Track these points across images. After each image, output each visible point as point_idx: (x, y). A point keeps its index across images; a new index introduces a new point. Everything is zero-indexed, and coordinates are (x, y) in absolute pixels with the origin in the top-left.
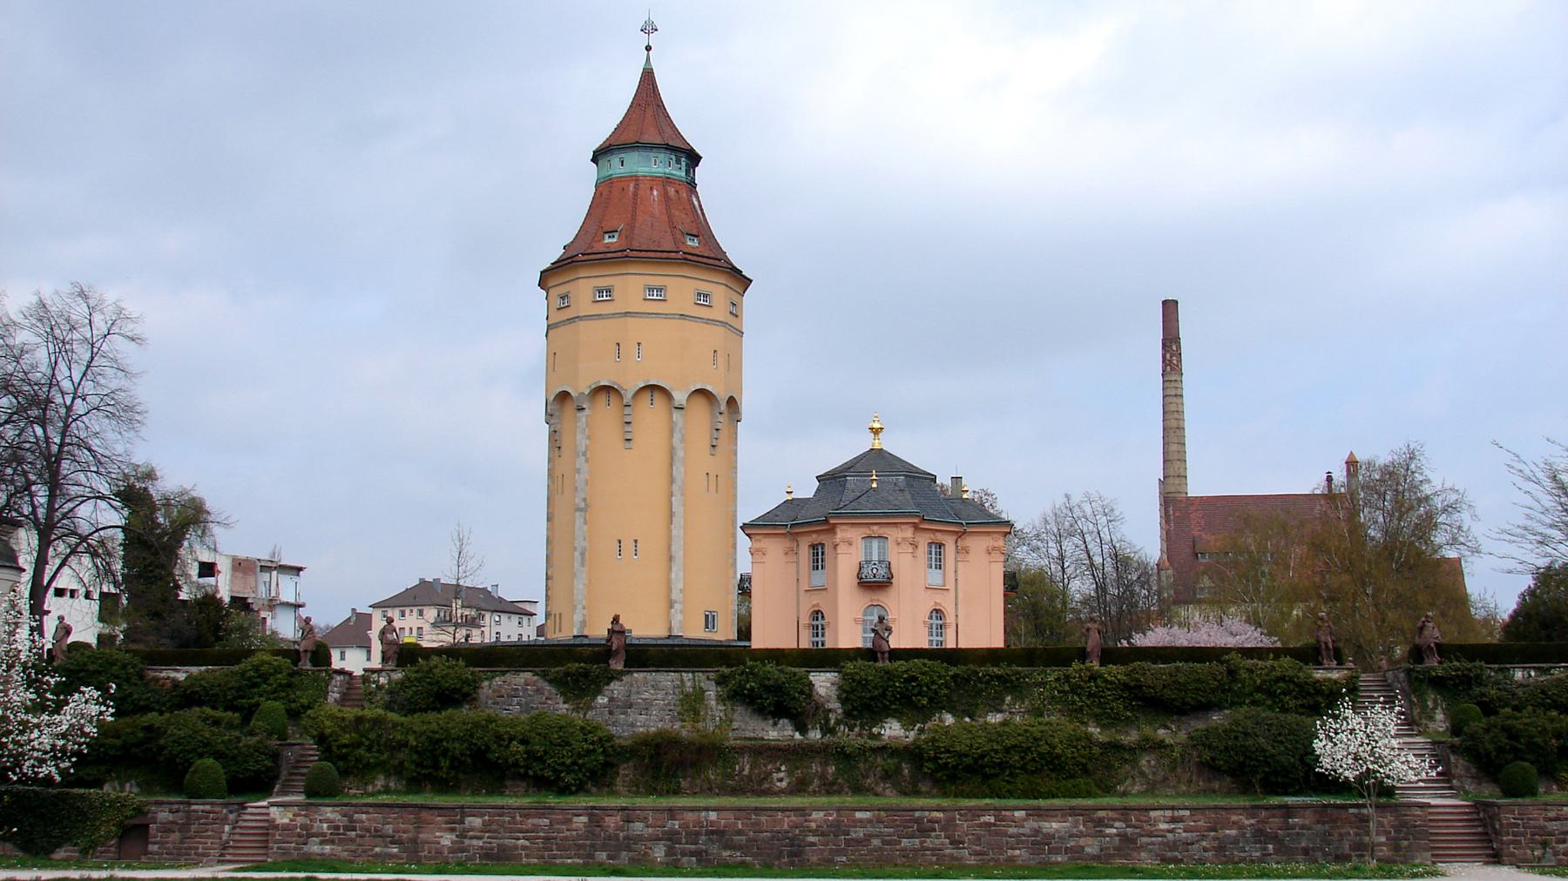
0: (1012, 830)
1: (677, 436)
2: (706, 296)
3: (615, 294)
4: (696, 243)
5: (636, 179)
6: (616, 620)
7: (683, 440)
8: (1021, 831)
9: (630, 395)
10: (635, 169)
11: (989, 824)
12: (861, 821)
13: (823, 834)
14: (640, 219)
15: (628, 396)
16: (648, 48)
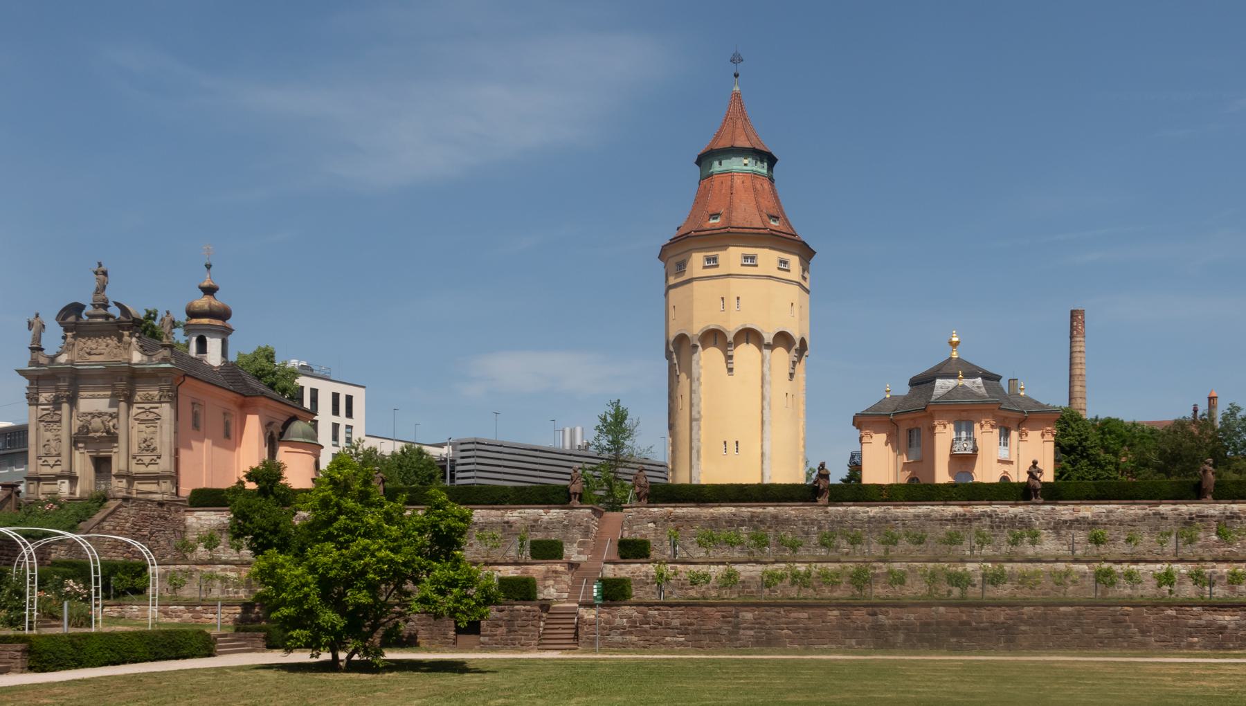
0: (1192, 622)
1: (766, 366)
2: (785, 263)
3: (720, 261)
4: (776, 224)
6: (822, 466)
7: (770, 369)
8: (1200, 622)
11: (1171, 617)
12: (1065, 614)
13: (1033, 624)
15: (730, 338)
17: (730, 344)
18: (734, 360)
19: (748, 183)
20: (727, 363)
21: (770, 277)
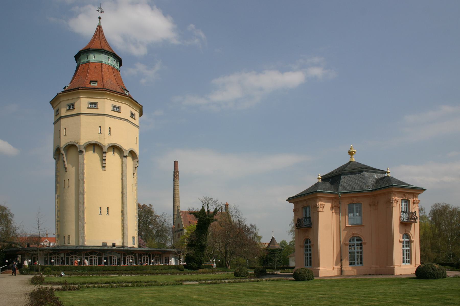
2: (133, 115)
3: (99, 106)
5: (101, 64)
9: (106, 148)
10: (100, 60)
15: (105, 150)
18: (107, 162)
19: (111, 70)
20: (102, 163)
21: (127, 120)
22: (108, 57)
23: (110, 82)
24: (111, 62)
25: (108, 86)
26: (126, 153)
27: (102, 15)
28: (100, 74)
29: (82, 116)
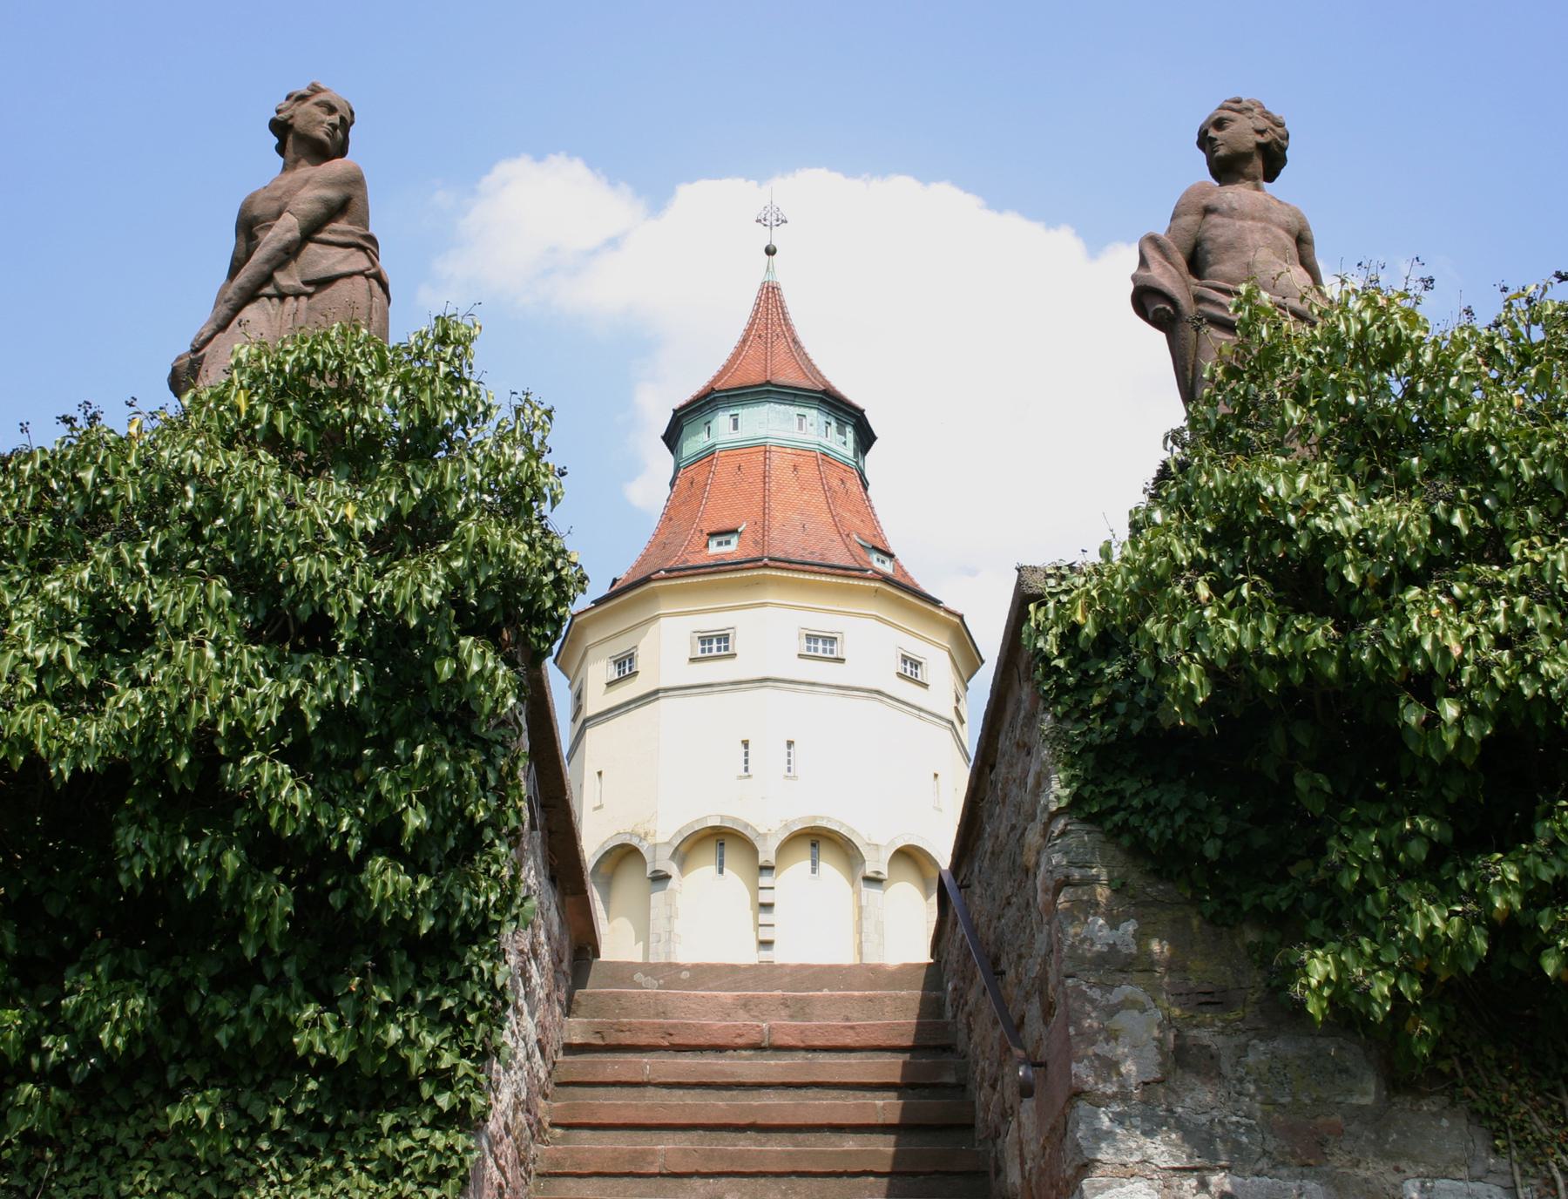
2: (916, 664)
3: (737, 645)
5: (763, 449)
10: (761, 433)
14: (777, 514)
15: (767, 854)
16: (770, 251)
17: (767, 869)
19: (808, 472)
22: (793, 411)
23: (799, 524)
24: (812, 429)
25: (785, 543)
26: (877, 863)
27: (779, 238)
28: (758, 498)
29: (663, 704)
